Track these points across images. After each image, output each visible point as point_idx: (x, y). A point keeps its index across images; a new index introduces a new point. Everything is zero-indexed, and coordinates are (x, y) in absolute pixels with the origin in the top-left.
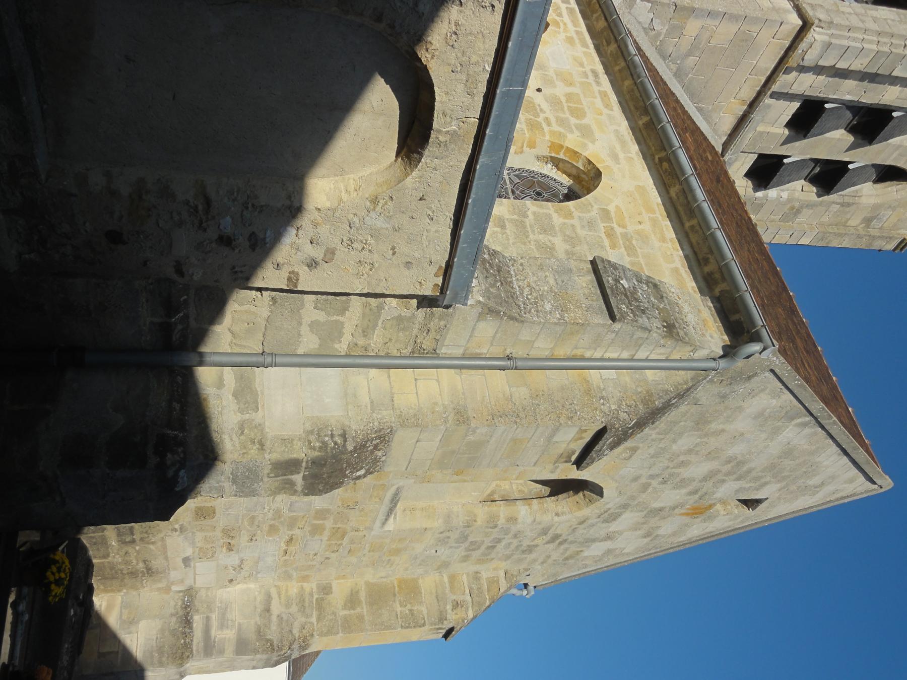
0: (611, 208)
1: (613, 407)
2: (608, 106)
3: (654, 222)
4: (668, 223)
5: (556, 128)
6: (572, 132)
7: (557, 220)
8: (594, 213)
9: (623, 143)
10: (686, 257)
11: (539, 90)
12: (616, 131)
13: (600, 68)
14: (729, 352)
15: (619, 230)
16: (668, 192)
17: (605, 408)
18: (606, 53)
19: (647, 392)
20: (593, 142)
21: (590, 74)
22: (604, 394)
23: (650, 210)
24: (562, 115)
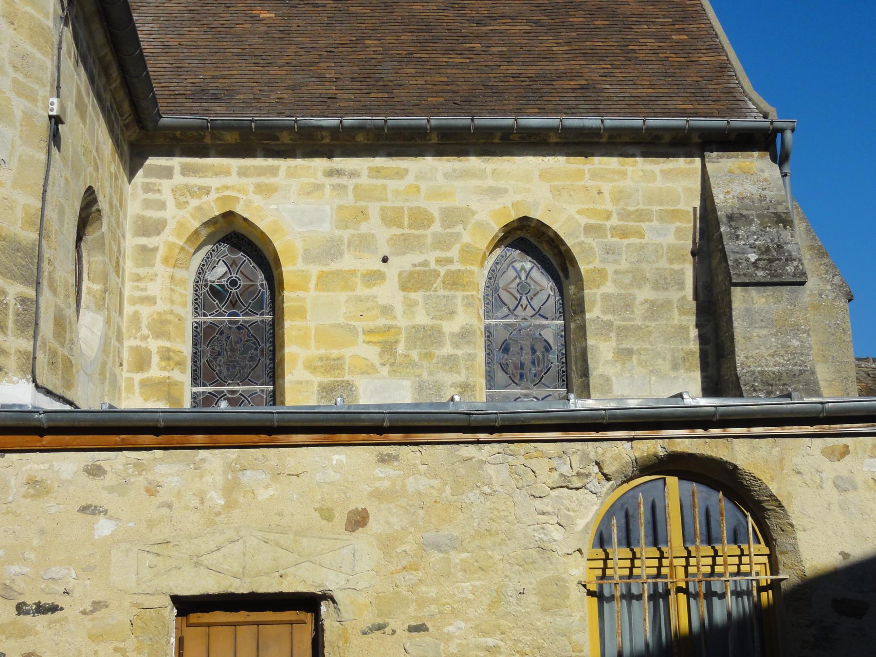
0: (583, 220)
1: (829, 287)
2: (400, 174)
3: (595, 175)
4: (596, 160)
5: (454, 252)
6: (458, 235)
7: (609, 288)
8: (592, 242)
9: (466, 174)
10: (645, 155)
11: (385, 260)
12: (446, 175)
13: (320, 164)
14: (781, 159)
15: (614, 221)
16: (548, 144)
17: (832, 296)
18: (285, 144)
19: (810, 249)
20: (473, 213)
21: (335, 180)
22: (816, 292)
23: (579, 174)
24: (429, 240)
